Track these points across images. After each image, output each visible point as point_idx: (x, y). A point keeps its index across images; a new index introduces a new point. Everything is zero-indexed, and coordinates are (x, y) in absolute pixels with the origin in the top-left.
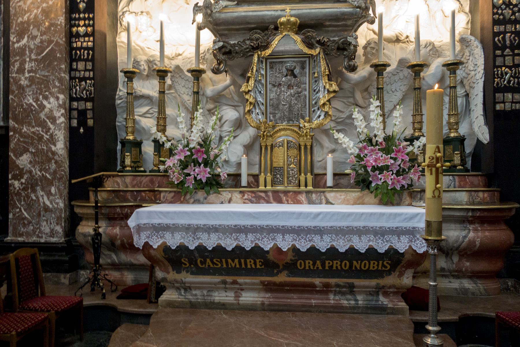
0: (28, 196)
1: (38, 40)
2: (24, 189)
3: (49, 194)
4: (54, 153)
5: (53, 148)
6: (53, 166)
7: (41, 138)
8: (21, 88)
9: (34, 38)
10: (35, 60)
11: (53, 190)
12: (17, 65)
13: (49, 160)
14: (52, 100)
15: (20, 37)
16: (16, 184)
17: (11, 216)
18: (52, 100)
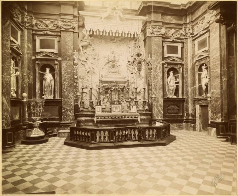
0: (66, 113)
1: (68, 83)
2: (65, 112)
3: (71, 113)
4: (71, 105)
5: (71, 104)
6: (71, 107)
7: (69, 102)
8: (64, 91)
9: (67, 82)
10: (67, 86)
11: (71, 112)
12: (63, 87)
13: (71, 106)
14: (71, 94)
15: (64, 81)
16: (64, 111)
17: (62, 117)
18: (71, 94)
